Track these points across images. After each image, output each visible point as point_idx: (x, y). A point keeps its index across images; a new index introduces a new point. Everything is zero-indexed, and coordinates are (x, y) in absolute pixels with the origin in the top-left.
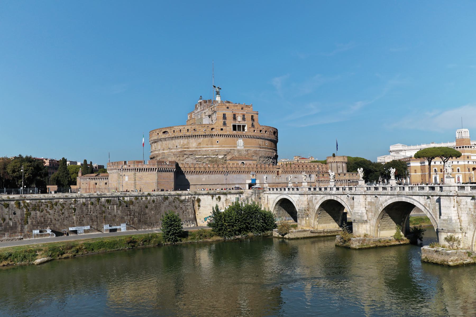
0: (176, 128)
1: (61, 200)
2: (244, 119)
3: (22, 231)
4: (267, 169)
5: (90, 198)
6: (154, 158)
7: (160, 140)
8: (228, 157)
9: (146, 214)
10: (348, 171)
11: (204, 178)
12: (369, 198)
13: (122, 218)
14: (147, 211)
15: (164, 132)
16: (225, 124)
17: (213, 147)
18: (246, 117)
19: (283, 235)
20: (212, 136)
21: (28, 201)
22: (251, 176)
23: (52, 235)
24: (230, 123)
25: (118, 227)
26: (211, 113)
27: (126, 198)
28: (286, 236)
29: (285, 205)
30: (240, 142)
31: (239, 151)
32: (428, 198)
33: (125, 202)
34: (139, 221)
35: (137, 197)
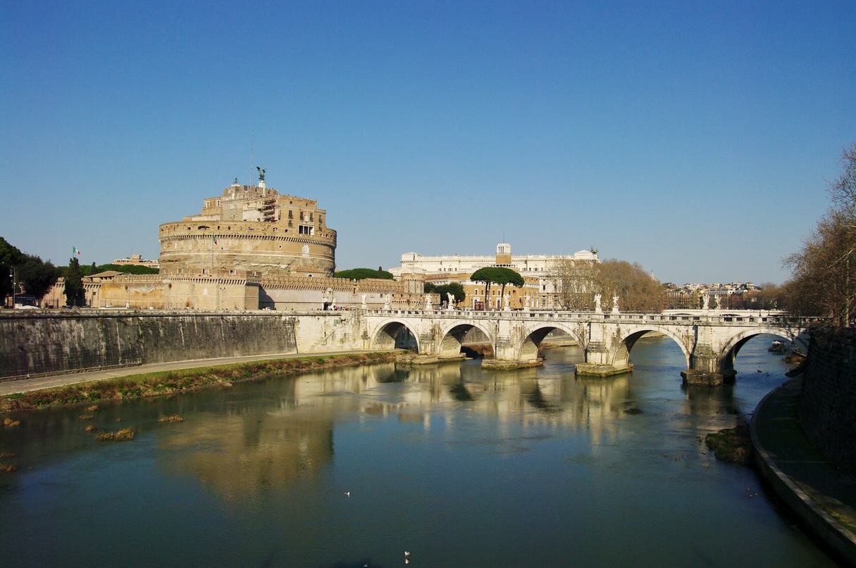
1: (170, 318)
2: (311, 219)
4: (344, 285)
5: (196, 316)
6: (176, 261)
8: (292, 267)
15: (200, 228)
16: (290, 224)
17: (274, 253)
18: (313, 216)
20: (273, 238)
21: (141, 318)
22: (328, 293)
24: (297, 223)
27: (228, 317)
30: (306, 248)
31: (304, 260)
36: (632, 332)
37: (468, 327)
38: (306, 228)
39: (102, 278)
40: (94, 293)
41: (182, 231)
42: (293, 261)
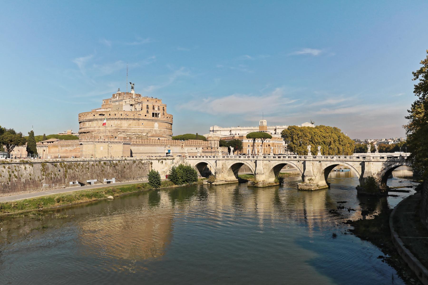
0: (112, 112)
2: (159, 109)
3: (64, 183)
7: (96, 120)
8: (149, 135)
9: (125, 172)
10: (220, 146)
11: (142, 149)
12: (265, 162)
13: (113, 174)
14: (125, 170)
16: (148, 112)
17: (139, 127)
19: (211, 183)
21: (65, 163)
23: (79, 185)
24: (151, 111)
25: (111, 180)
26: (134, 103)
28: (214, 183)
29: (202, 166)
30: (156, 125)
31: (155, 131)
32: (299, 162)
33: (113, 164)
34: (122, 176)
35: (119, 161)
36: (328, 166)
37: (241, 164)
38: (156, 114)
39: (48, 142)
40: (44, 151)
41: (91, 117)
42: (150, 131)
